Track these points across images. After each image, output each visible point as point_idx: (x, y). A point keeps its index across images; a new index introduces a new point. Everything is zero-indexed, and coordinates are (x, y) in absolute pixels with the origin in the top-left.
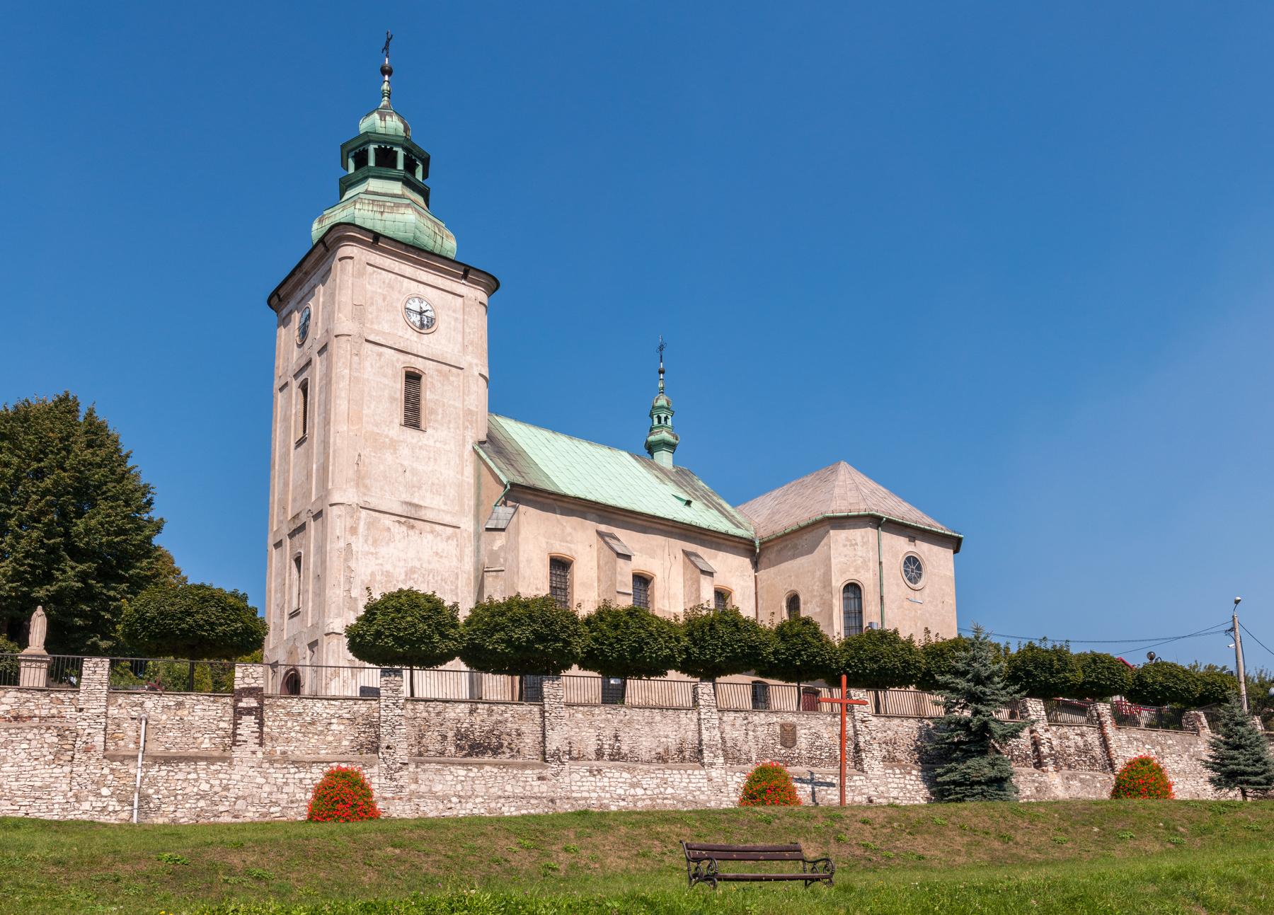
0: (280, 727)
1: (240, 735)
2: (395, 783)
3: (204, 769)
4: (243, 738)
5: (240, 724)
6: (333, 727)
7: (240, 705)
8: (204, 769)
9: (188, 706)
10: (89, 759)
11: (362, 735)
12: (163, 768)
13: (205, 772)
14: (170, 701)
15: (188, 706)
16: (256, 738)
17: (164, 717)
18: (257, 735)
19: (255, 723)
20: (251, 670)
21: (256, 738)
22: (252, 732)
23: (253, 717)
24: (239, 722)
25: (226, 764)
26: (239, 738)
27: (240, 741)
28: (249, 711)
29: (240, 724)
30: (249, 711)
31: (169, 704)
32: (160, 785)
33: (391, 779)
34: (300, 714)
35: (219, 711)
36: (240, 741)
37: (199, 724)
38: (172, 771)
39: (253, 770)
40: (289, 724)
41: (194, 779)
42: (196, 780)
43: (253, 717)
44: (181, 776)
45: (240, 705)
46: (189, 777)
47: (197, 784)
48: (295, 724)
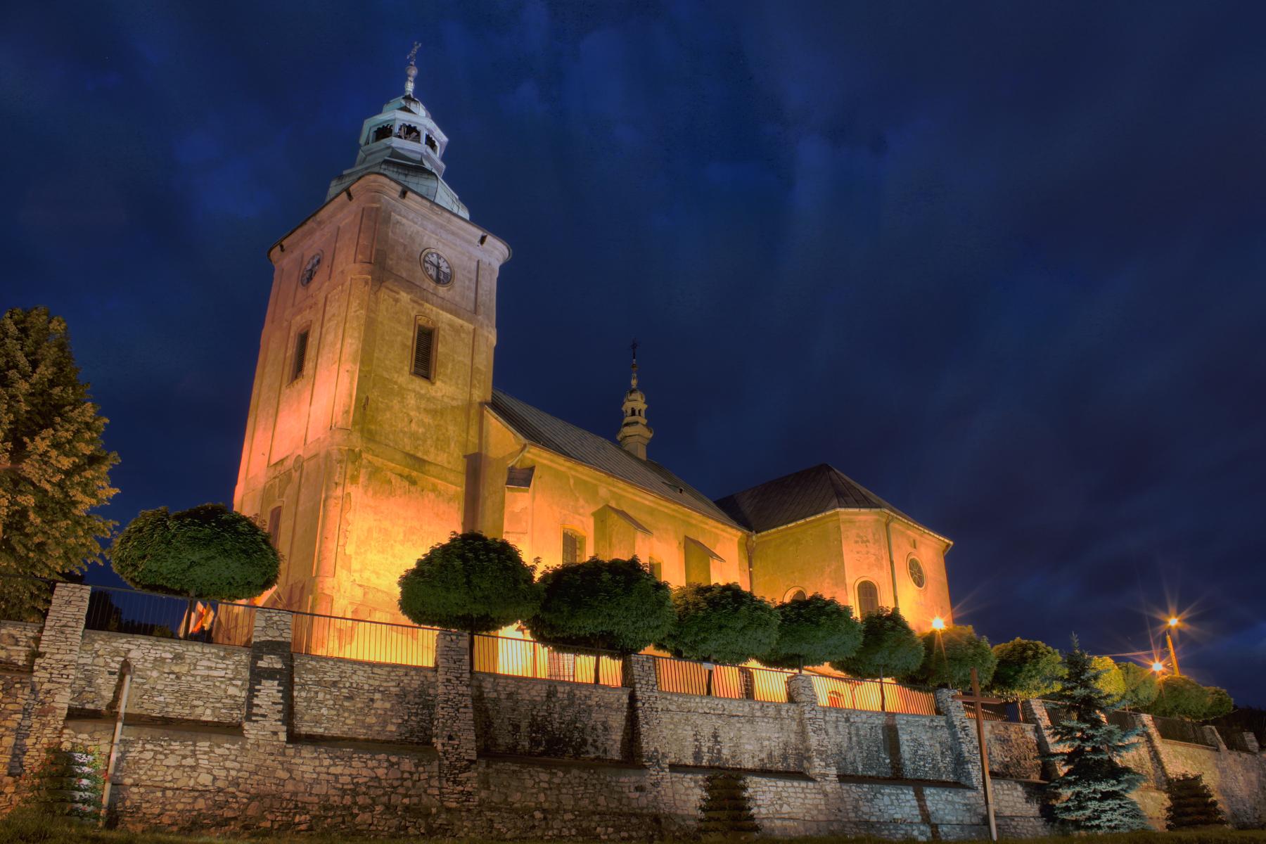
0: (308, 700)
1: (257, 705)
2: (460, 788)
3: (205, 753)
4: (262, 711)
5: (259, 691)
6: (378, 704)
7: (261, 664)
8: (205, 753)
9: (188, 661)
10: (44, 726)
11: (413, 718)
12: (148, 746)
13: (206, 757)
14: (166, 651)
15: (188, 661)
16: (279, 712)
17: (155, 674)
18: (280, 707)
19: (279, 691)
20: (276, 618)
21: (279, 712)
22: (274, 703)
23: (276, 683)
24: (257, 687)
25: (236, 746)
26: (255, 710)
27: (256, 715)
28: (271, 674)
29: (259, 691)
30: (271, 674)
31: (163, 655)
32: (141, 772)
33: (454, 782)
34: (334, 684)
35: (229, 671)
36: (256, 715)
37: (200, 686)
38: (161, 753)
39: (272, 758)
40: (321, 696)
41: (191, 767)
42: (193, 768)
43: (276, 683)
44: (171, 761)
45: (261, 664)
46: (184, 762)
47: (195, 774)
48: (328, 697)
